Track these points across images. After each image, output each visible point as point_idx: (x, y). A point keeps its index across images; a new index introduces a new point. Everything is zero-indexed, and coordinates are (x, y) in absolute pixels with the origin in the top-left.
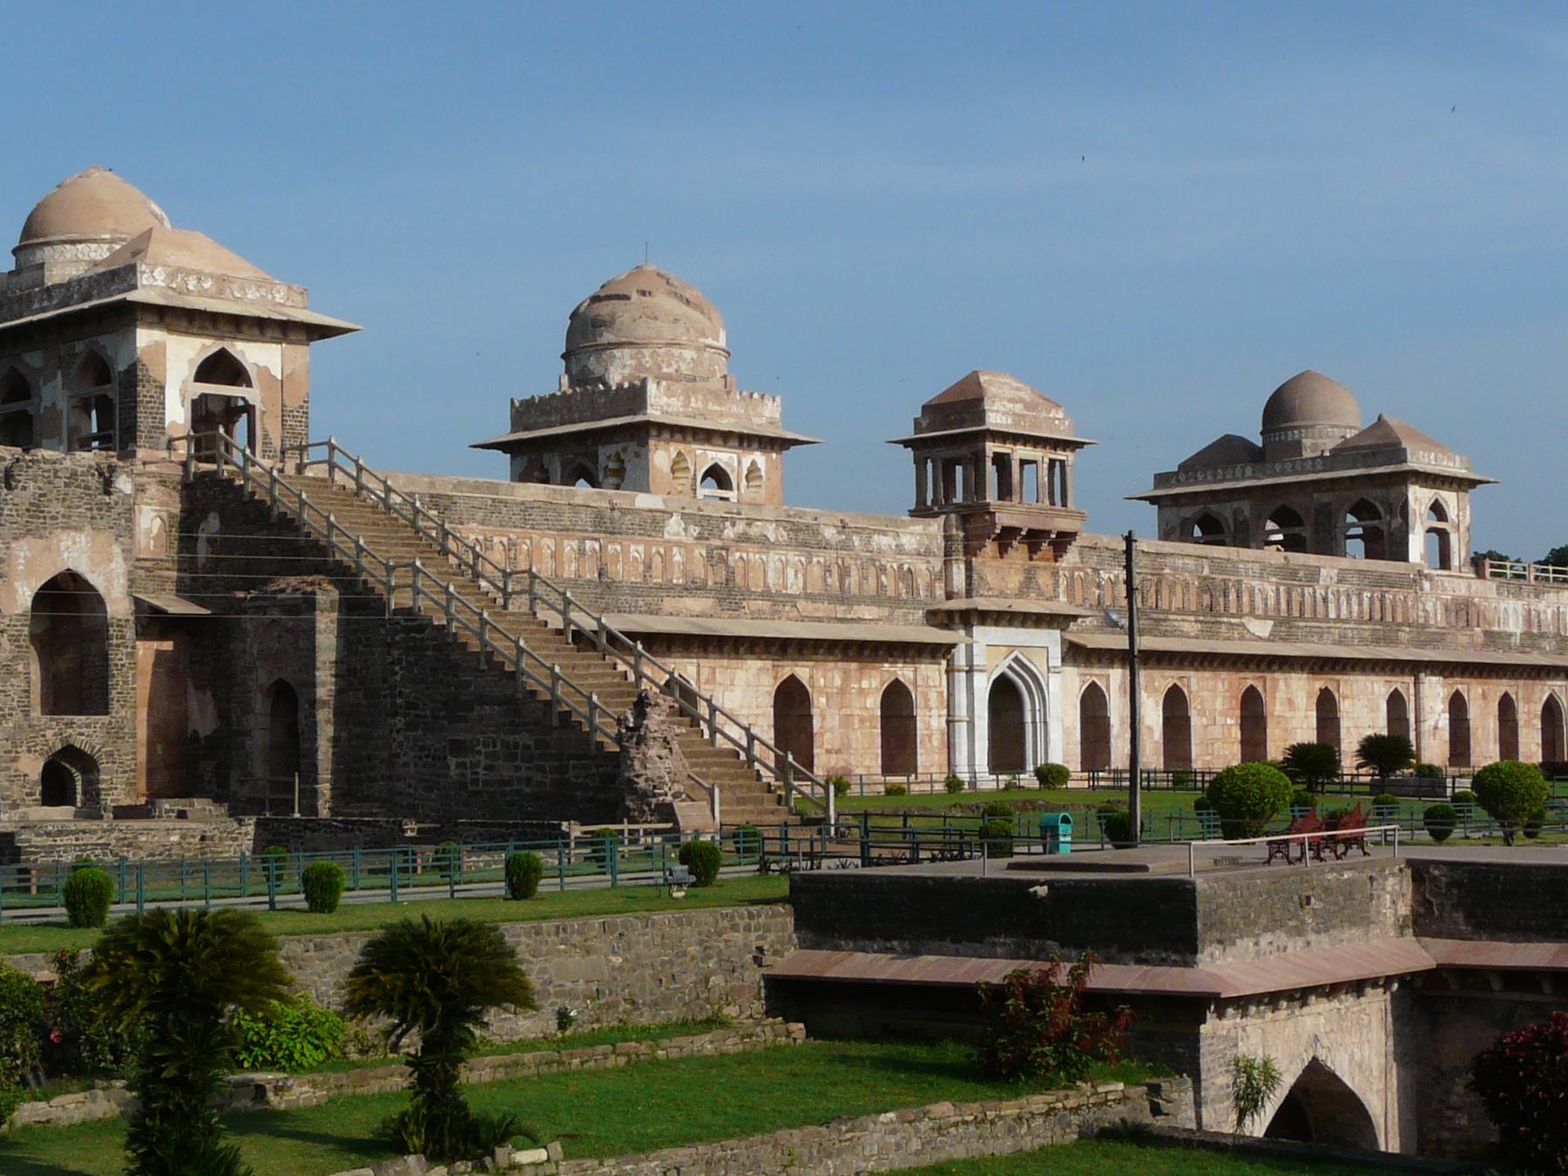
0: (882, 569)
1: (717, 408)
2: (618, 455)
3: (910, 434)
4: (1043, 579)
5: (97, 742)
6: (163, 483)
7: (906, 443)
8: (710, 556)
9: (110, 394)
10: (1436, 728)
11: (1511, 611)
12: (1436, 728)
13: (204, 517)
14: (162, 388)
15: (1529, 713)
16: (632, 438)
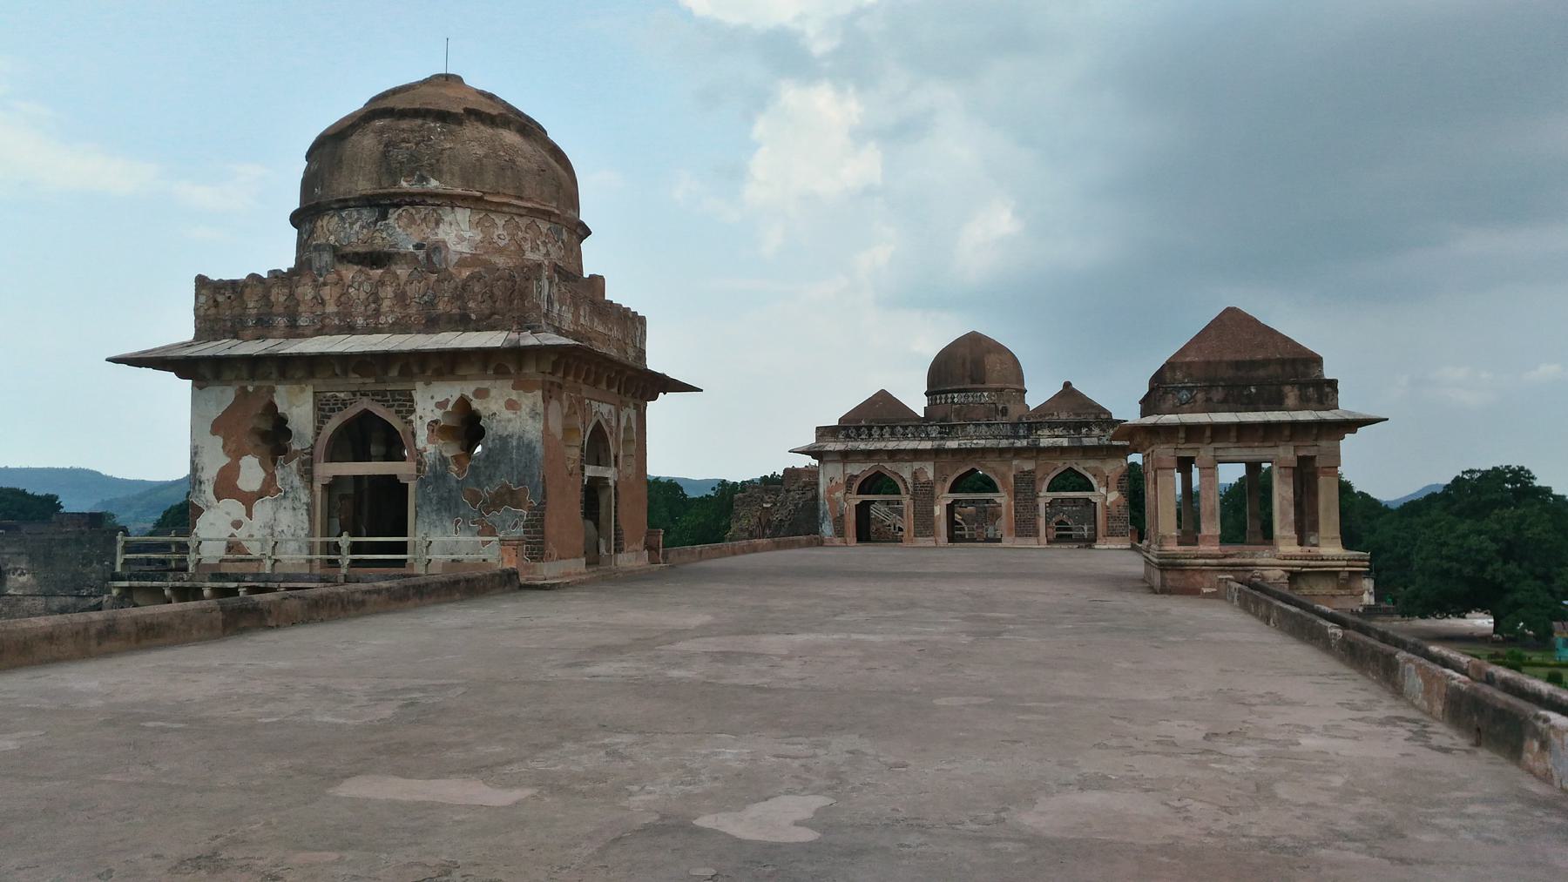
1: (600, 329)
2: (463, 403)
16: (501, 373)
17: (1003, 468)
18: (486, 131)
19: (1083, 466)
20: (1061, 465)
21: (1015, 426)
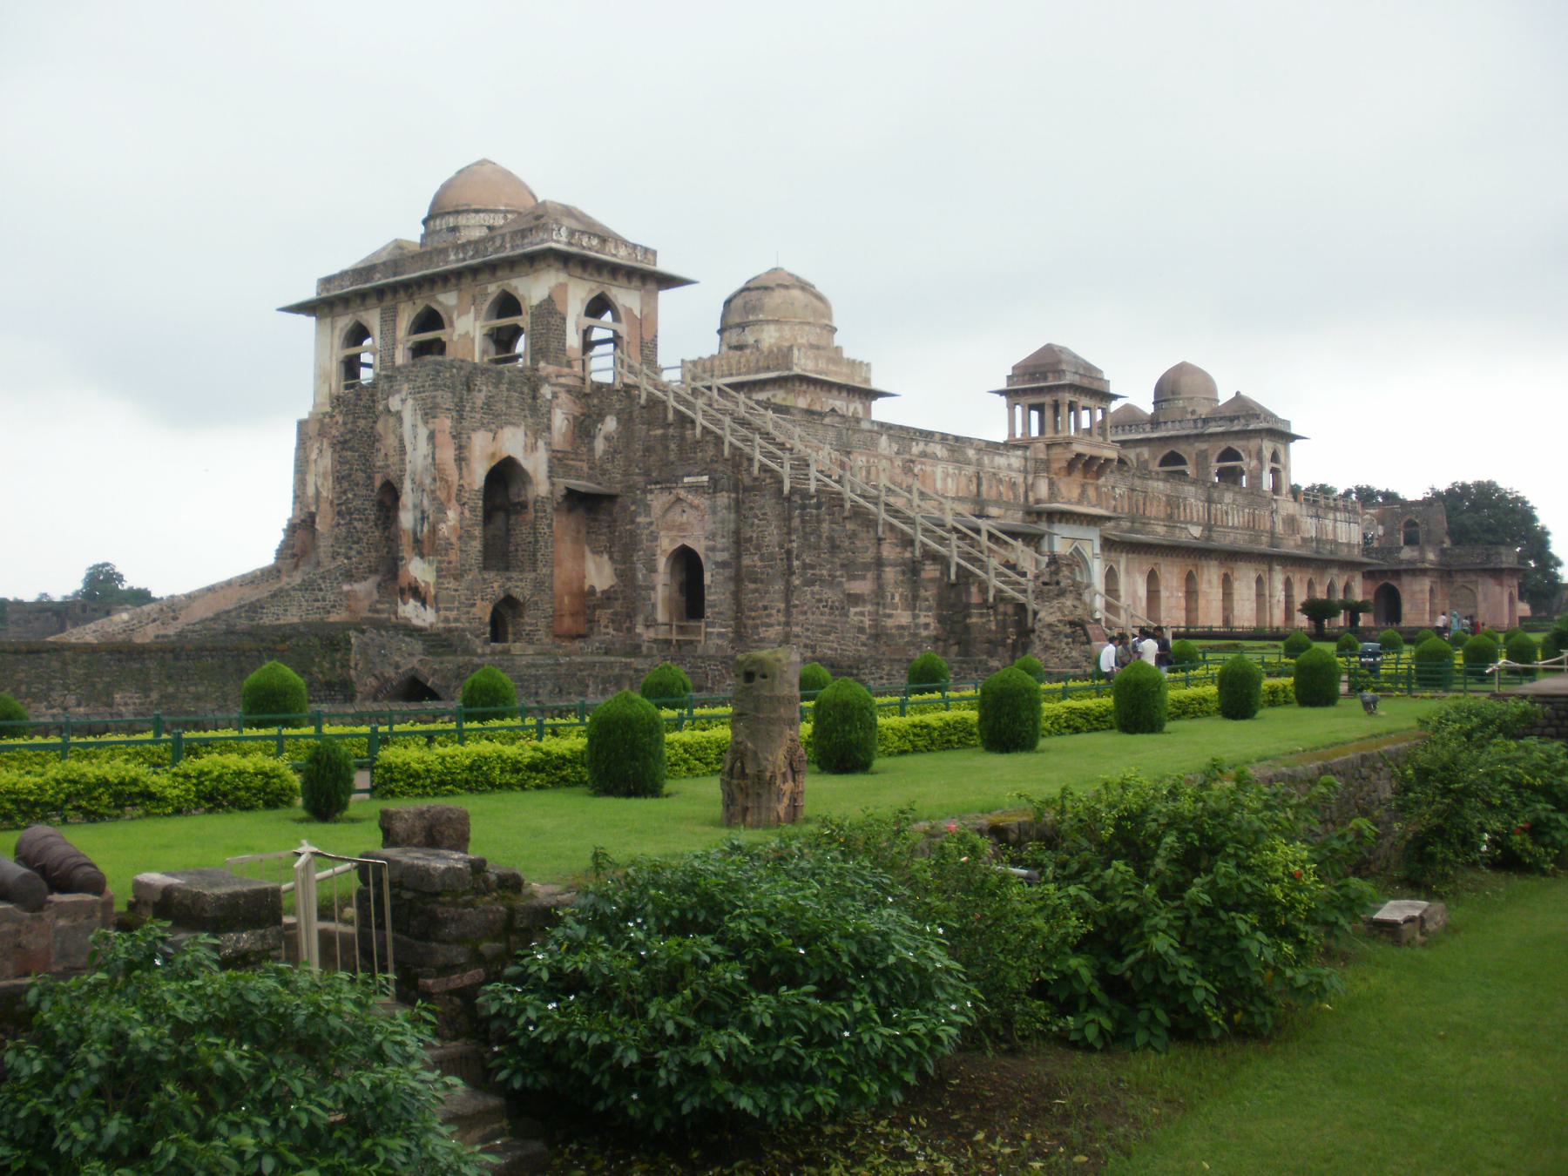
0: (1000, 481)
3: (1003, 385)
4: (1091, 492)
5: (527, 593)
6: (569, 392)
7: (1001, 393)
8: (904, 468)
9: (522, 325)
13: (601, 418)
14: (564, 319)
16: (780, 387)
17: (1189, 449)
18: (783, 292)
19: (1237, 445)
20: (1223, 445)
21: (1195, 421)
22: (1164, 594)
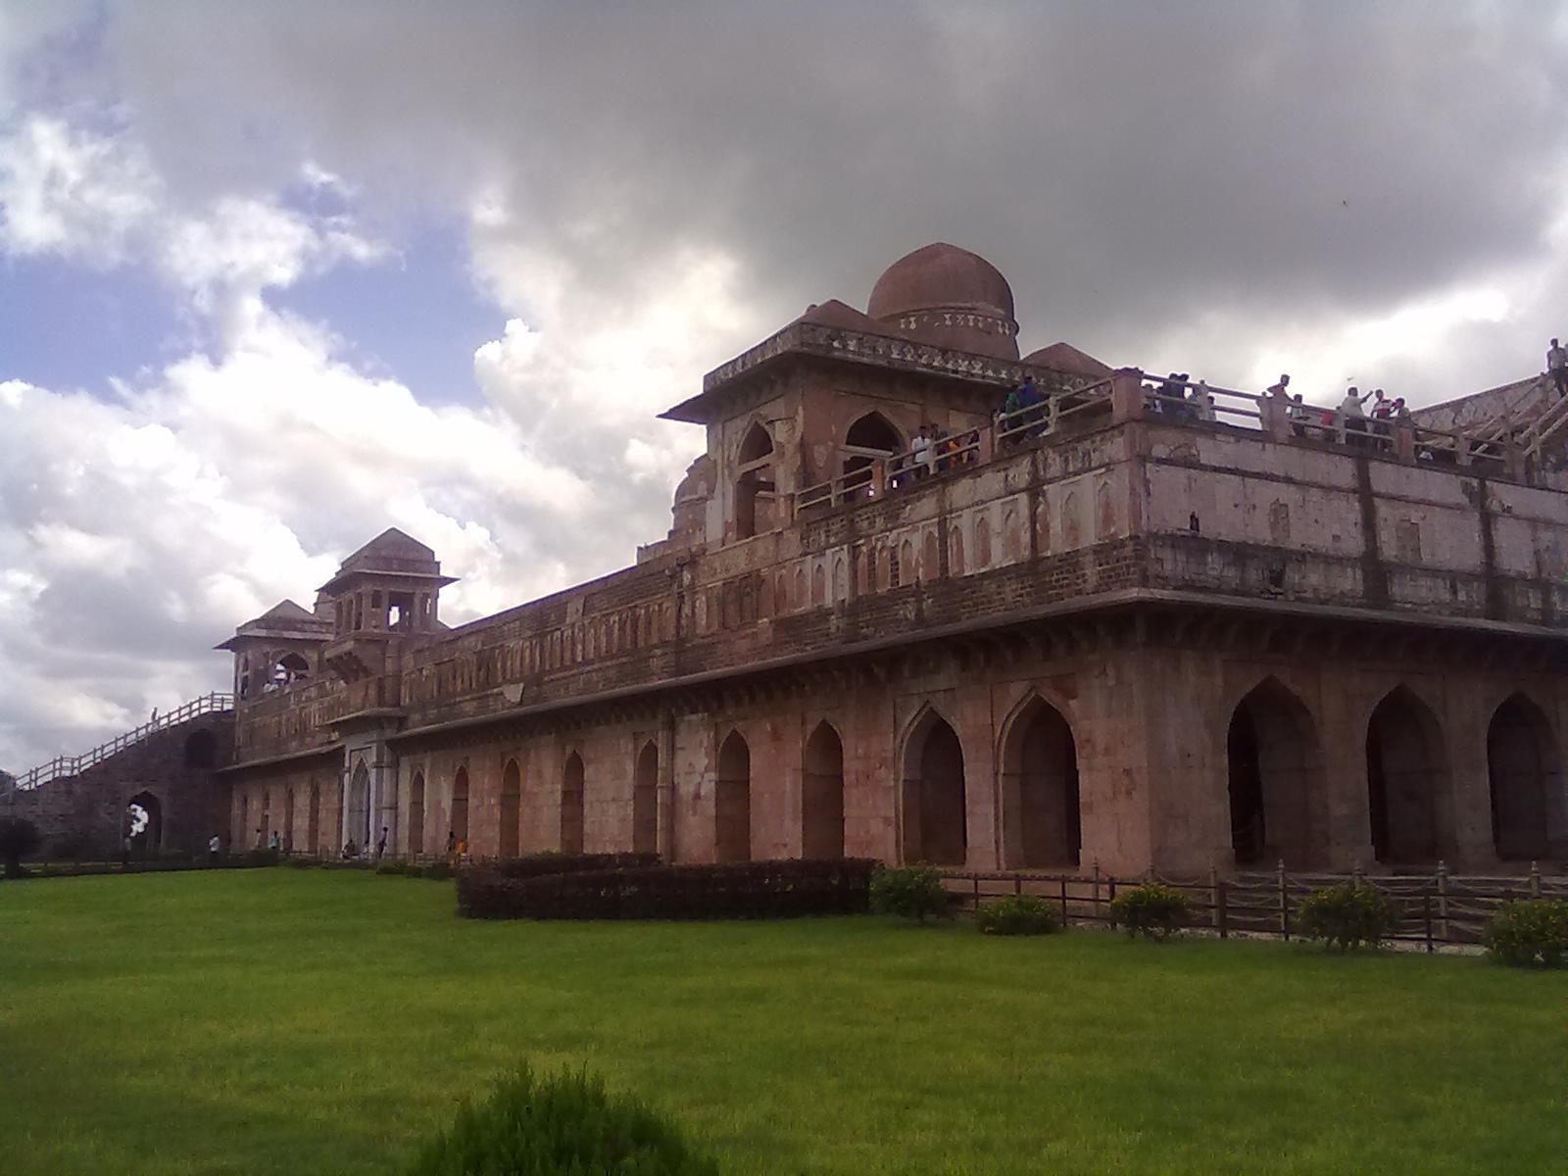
10: (697, 796)
11: (828, 569)
12: (697, 796)
15: (867, 757)
22: (472, 802)
